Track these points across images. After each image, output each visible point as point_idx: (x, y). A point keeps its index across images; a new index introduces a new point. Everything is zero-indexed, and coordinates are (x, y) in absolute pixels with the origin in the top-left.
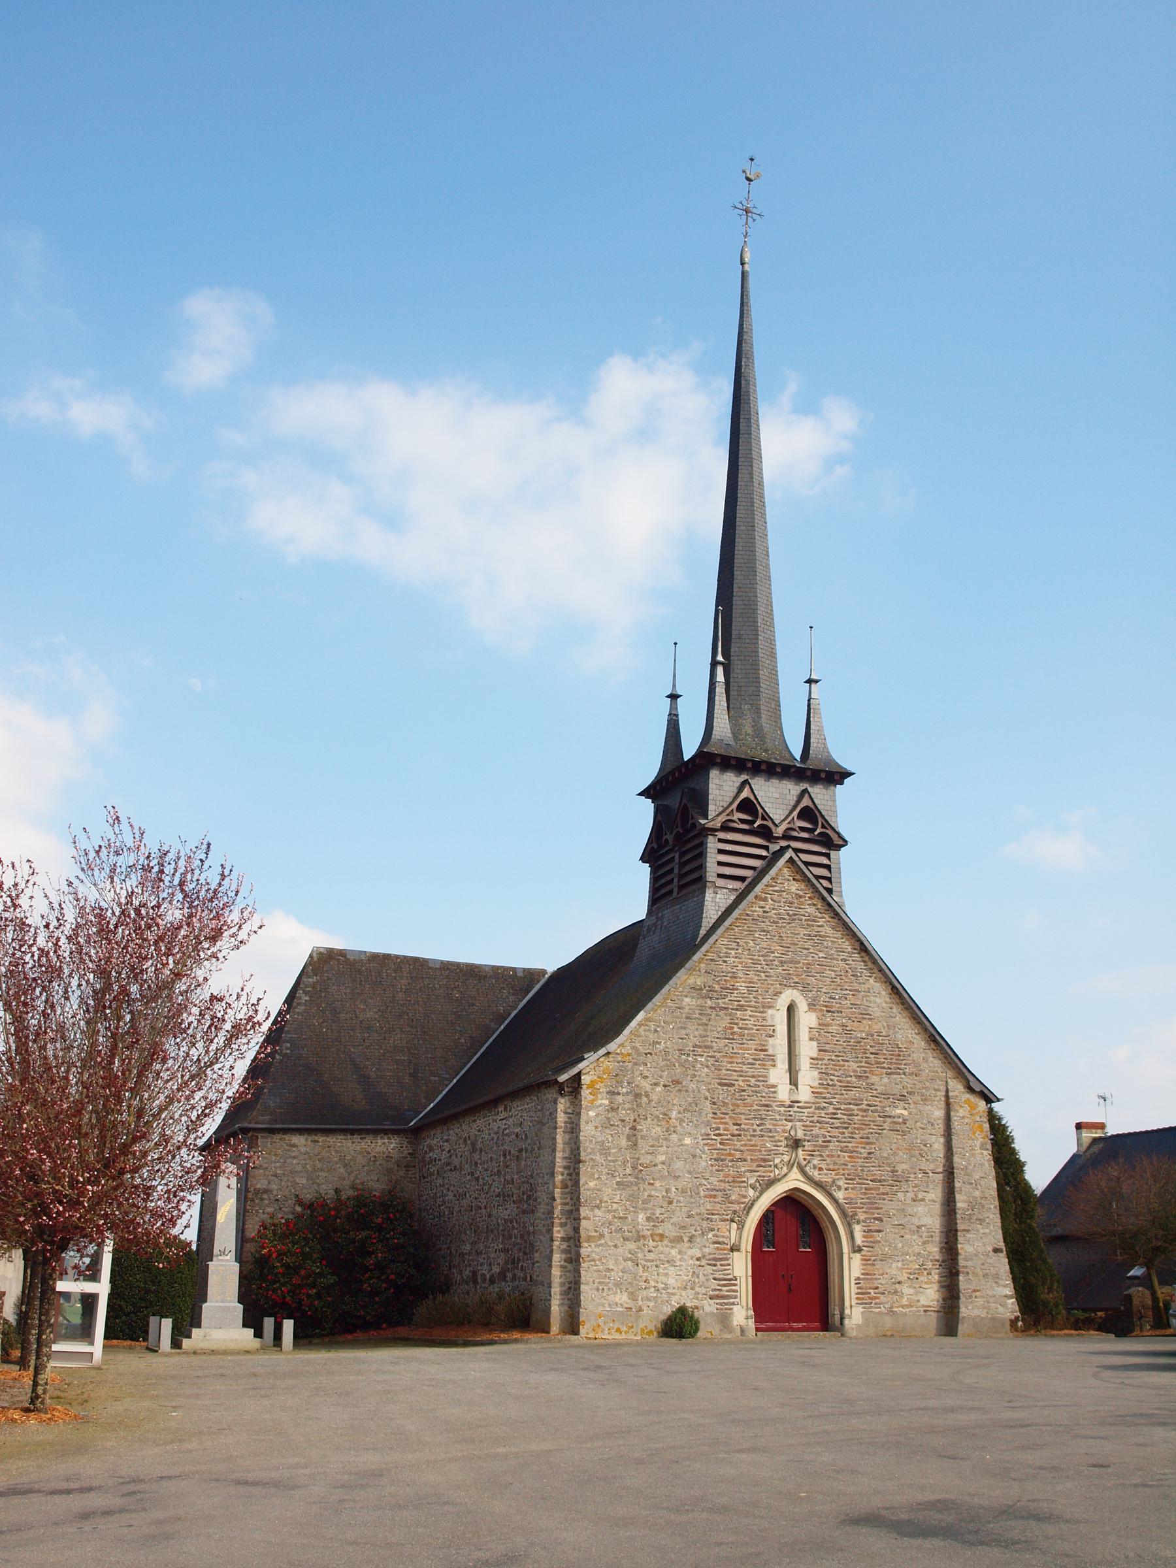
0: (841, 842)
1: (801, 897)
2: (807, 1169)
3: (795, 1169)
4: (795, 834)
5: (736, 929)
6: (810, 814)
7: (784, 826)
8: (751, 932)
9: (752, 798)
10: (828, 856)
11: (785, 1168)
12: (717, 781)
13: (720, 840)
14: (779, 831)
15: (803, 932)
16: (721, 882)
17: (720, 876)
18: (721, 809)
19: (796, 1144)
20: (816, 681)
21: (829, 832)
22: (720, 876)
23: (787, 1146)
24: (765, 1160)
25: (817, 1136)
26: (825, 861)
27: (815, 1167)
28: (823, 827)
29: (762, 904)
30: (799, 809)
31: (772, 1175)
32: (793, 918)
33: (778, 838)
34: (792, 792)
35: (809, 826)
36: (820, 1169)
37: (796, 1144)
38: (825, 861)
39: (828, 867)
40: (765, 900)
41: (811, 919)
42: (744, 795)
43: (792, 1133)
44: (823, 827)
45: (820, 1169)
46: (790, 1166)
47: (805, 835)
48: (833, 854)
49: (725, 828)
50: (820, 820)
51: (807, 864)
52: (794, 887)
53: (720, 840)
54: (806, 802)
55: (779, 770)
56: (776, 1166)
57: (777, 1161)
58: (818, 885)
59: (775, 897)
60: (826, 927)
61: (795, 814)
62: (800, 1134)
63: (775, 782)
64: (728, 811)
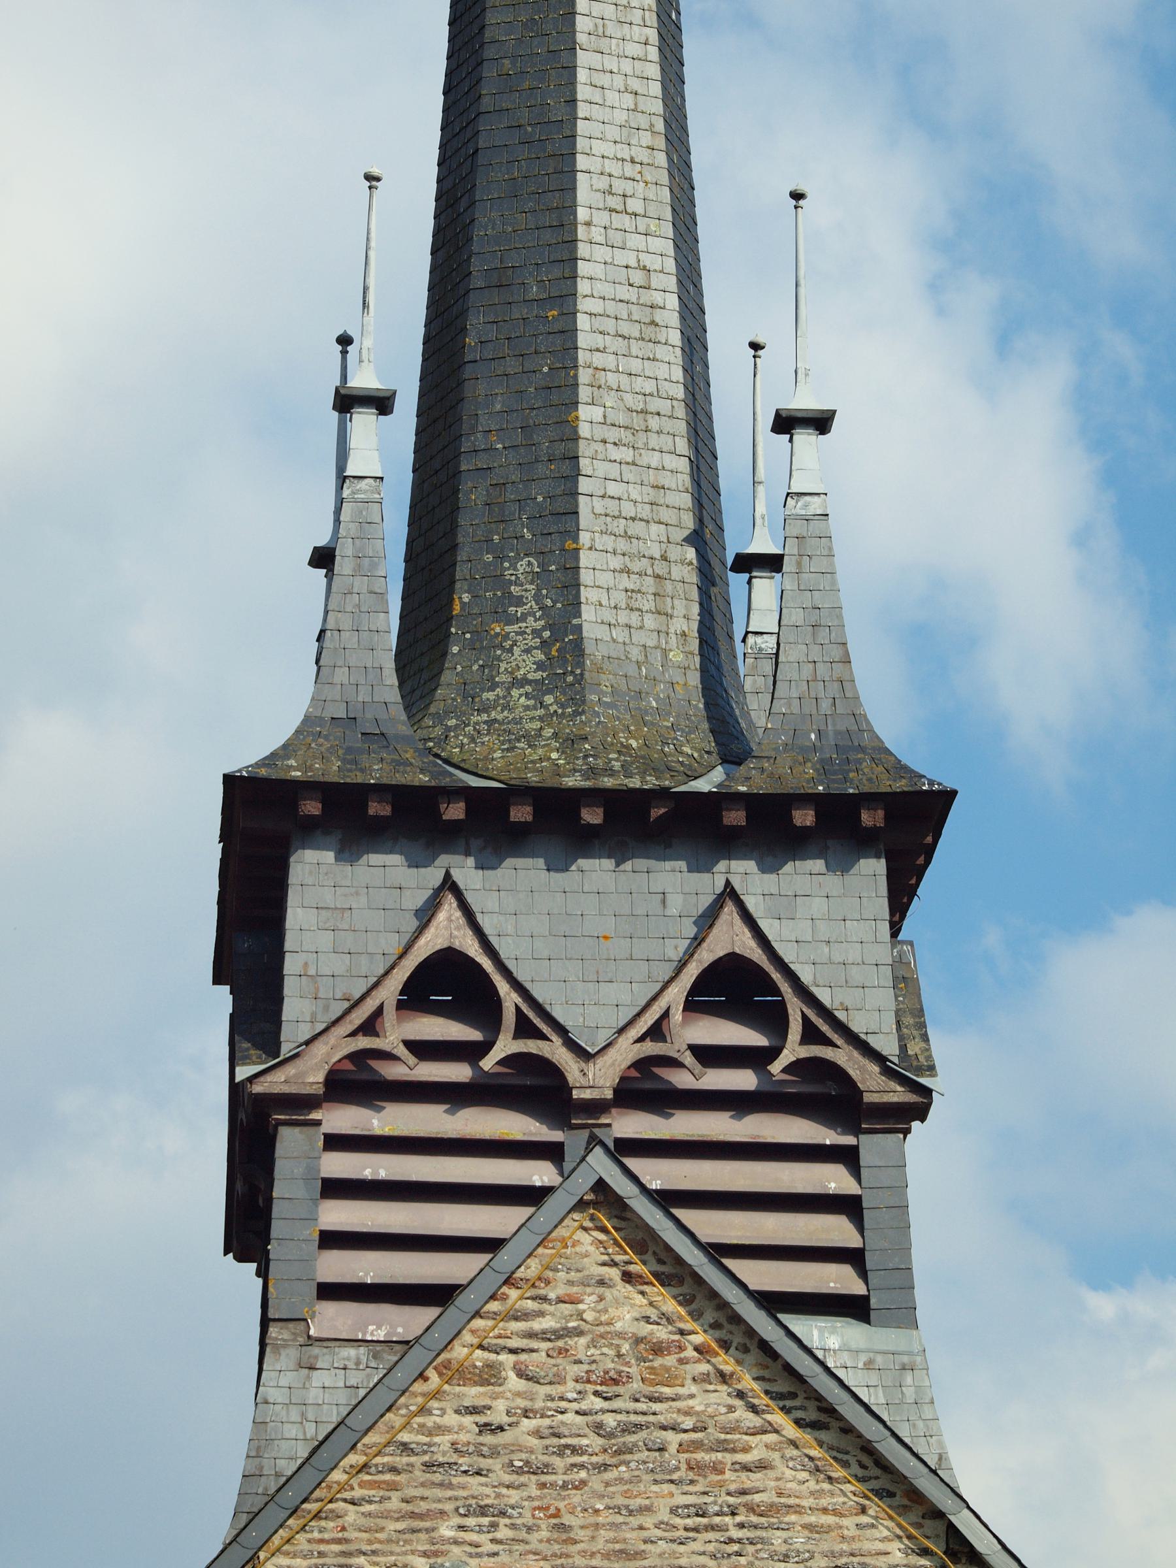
0: (898, 1094)
1: (658, 1349)
4: (682, 1080)
5: (352, 1515)
6: (736, 986)
7: (625, 1053)
8: (419, 1519)
9: (473, 949)
10: (848, 1157)
12: (328, 897)
13: (336, 1142)
14: (593, 1080)
15: (664, 1498)
16: (333, 1318)
17: (330, 1292)
18: (338, 1008)
20: (821, 423)
21: (843, 1056)
22: (330, 1292)
26: (832, 1179)
28: (811, 1035)
29: (473, 1394)
30: (692, 971)
32: (619, 1444)
33: (596, 1107)
34: (676, 904)
35: (473, 1035)
38: (832, 1179)
39: (849, 1206)
40: (489, 1376)
41: (707, 1446)
42: (431, 942)
44: (524, 1029)
47: (743, 1080)
48: (872, 1147)
49: (356, 1082)
50: (795, 1009)
51: (668, 1199)
52: (632, 1309)
53: (336, 1142)
54: (729, 937)
55: (312, 807)
58: (731, 1294)
59: (536, 1361)
60: (785, 1466)
61: (676, 994)
63: (596, 872)
64: (359, 1017)
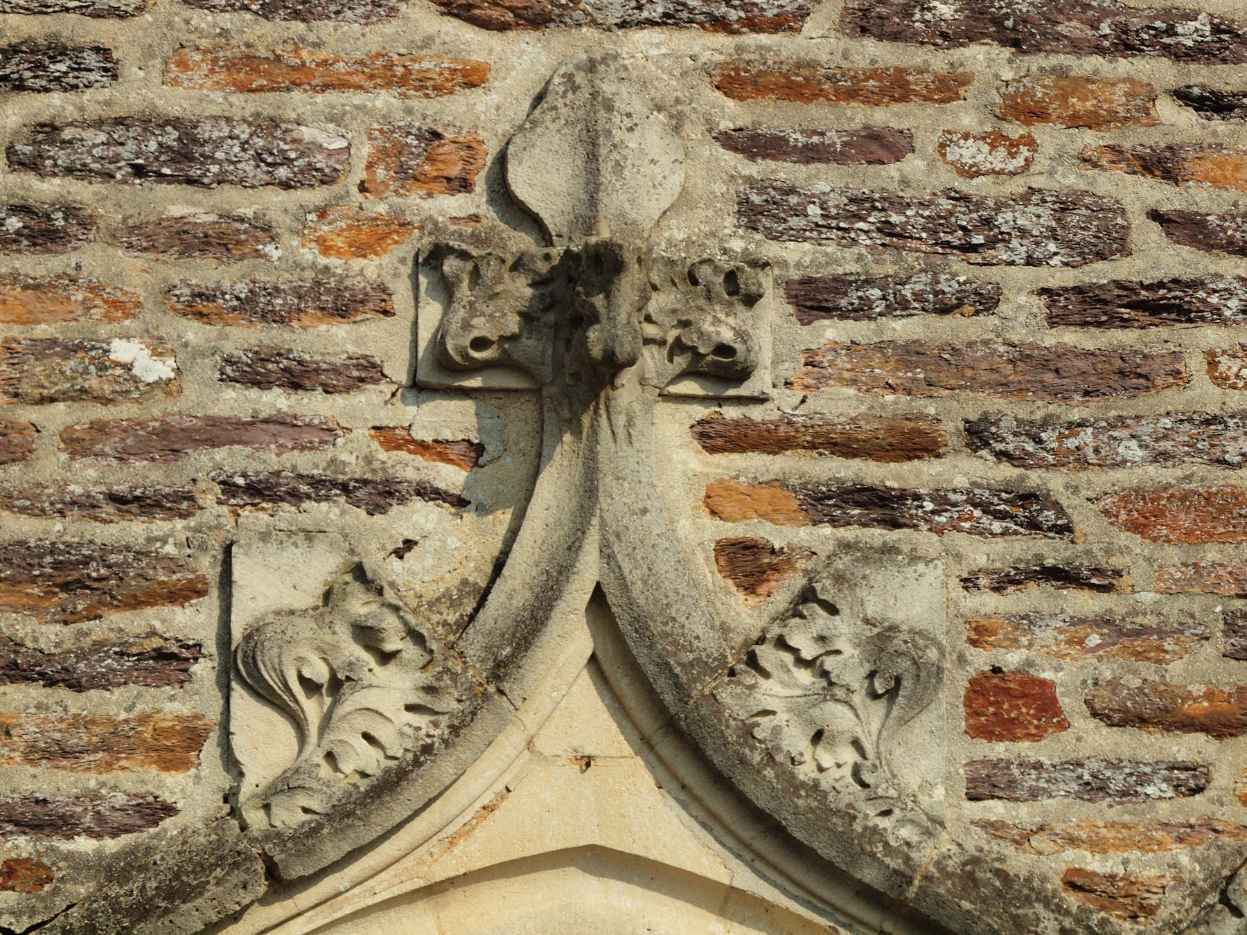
2: (776, 698)
3: (562, 685)
11: (389, 697)
19: (557, 338)
23: (438, 374)
24: (73, 579)
25: (969, 230)
27: (896, 674)
31: (193, 793)
36: (1008, 703)
37: (557, 338)
43: (544, 181)
45: (1008, 703)
46: (479, 662)
56: (241, 666)
57: (276, 579)
62: (669, 192)
